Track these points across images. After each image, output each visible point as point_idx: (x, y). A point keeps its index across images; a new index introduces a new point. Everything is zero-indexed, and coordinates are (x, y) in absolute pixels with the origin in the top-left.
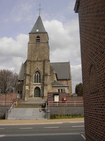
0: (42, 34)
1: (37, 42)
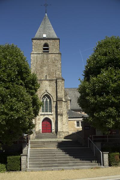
0: (51, 41)
1: (44, 52)
